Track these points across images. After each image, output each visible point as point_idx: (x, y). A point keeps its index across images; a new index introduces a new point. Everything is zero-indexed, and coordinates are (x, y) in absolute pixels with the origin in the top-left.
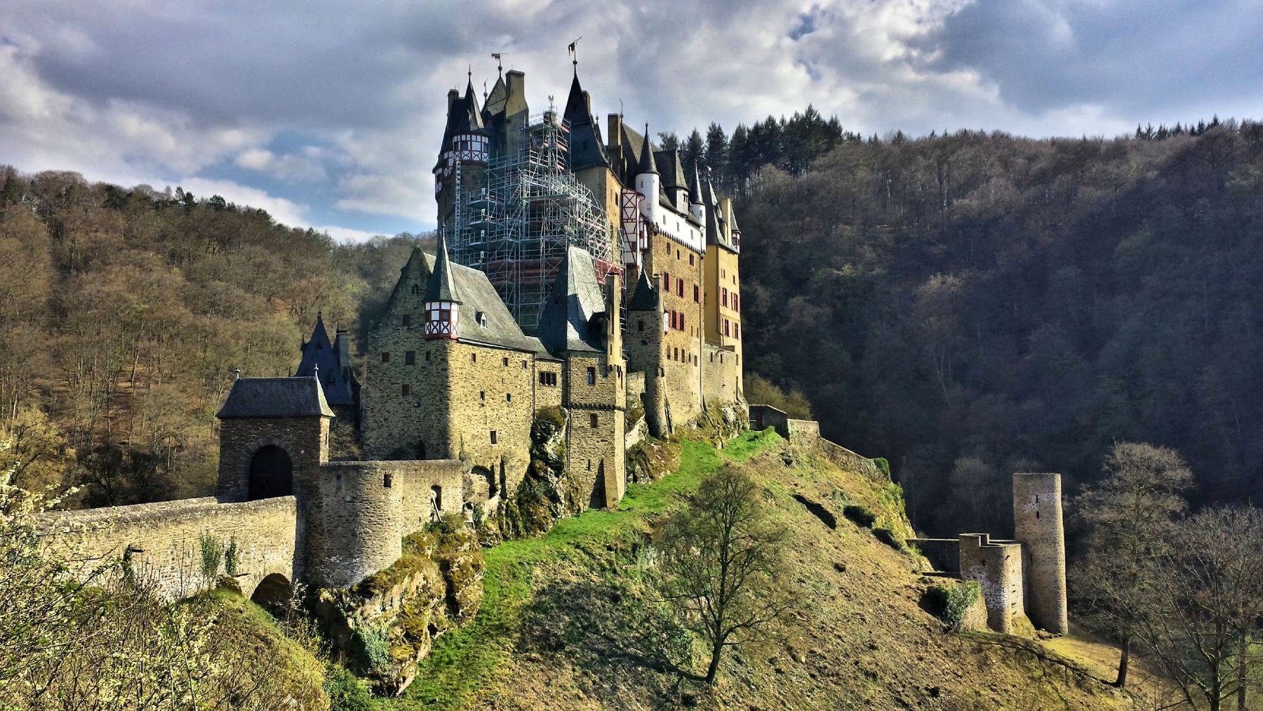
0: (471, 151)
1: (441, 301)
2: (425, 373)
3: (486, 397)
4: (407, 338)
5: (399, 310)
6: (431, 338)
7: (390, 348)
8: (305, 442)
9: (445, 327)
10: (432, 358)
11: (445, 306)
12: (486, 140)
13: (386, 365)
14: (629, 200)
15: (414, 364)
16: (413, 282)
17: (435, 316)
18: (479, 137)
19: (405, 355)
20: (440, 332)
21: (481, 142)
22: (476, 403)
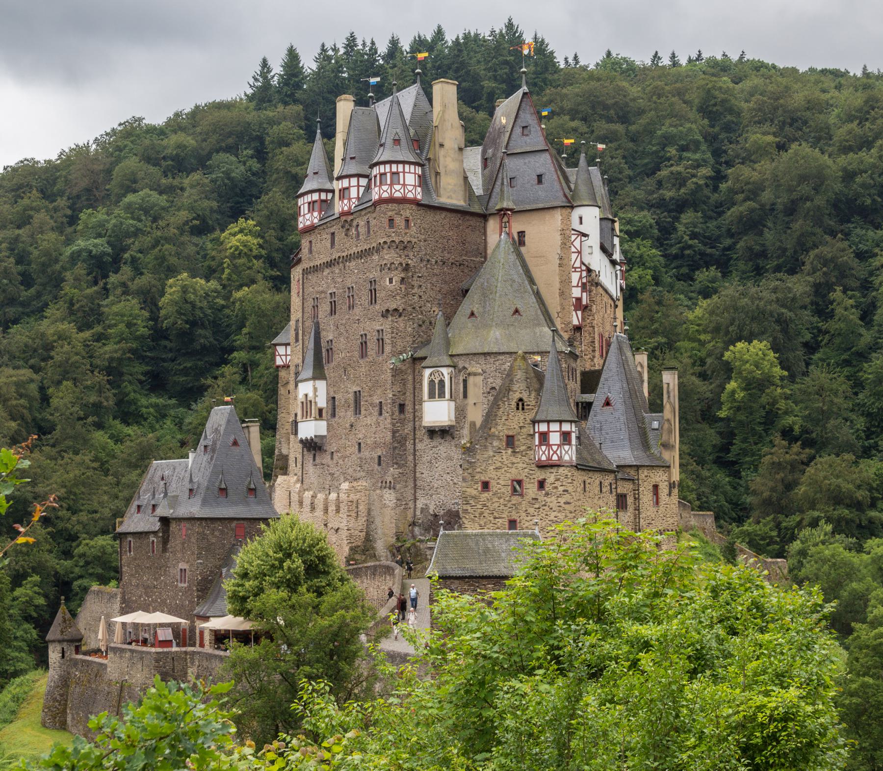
0: (404, 185)
1: (561, 422)
2: (537, 506)
4: (513, 463)
5: (501, 429)
6: (542, 466)
7: (490, 475)
9: (567, 452)
10: (548, 487)
11: (566, 427)
12: (419, 170)
13: (486, 495)
15: (522, 495)
16: (517, 396)
17: (555, 438)
18: (412, 167)
19: (510, 482)
20: (560, 458)
21: (415, 173)
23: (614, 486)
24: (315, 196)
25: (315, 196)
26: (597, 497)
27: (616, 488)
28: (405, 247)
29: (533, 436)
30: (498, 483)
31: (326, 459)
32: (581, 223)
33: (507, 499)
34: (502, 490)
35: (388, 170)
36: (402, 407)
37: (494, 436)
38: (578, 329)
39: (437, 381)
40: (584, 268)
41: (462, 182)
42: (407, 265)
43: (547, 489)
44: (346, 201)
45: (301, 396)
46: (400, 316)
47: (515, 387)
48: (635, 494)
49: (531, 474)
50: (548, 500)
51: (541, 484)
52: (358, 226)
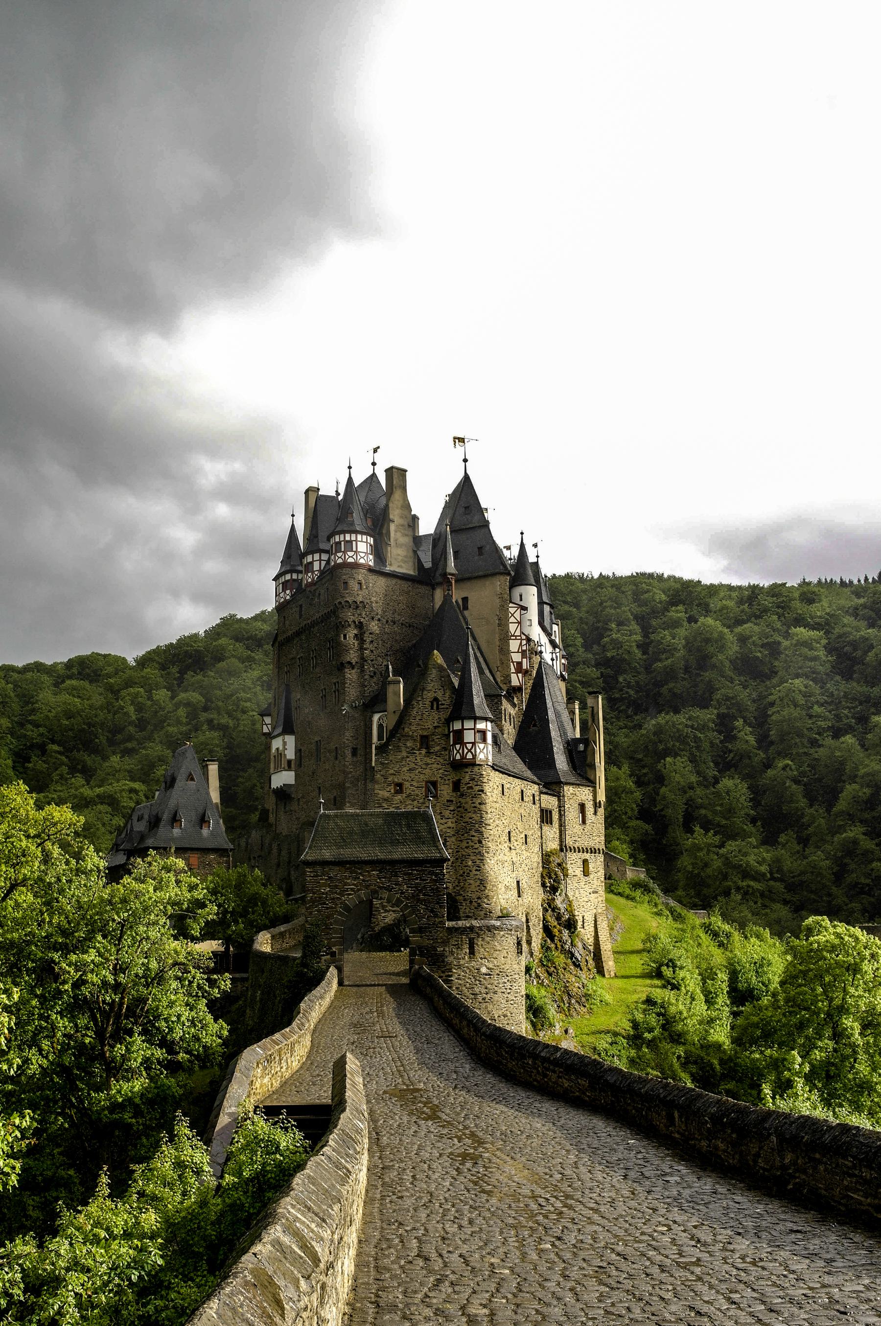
0: (356, 552)
1: (475, 719)
2: (452, 808)
3: (512, 839)
4: (427, 764)
5: (414, 728)
8: (424, 895)
10: (464, 788)
11: (481, 725)
12: (371, 540)
13: (399, 797)
14: (512, 615)
17: (469, 737)
18: (364, 537)
21: (367, 542)
22: (506, 845)
23: (537, 798)
24: (288, 577)
25: (288, 577)
26: (518, 805)
27: (540, 800)
28: (357, 607)
29: (448, 736)
30: (411, 785)
31: (294, 806)
32: (521, 600)
33: (421, 801)
34: (416, 792)
35: (342, 539)
36: (354, 752)
37: (409, 736)
38: (519, 689)
39: (384, 725)
40: (524, 637)
41: (411, 554)
42: (360, 623)
43: (462, 790)
44: (309, 574)
45: (273, 750)
46: (353, 668)
47: (430, 686)
48: (560, 811)
49: (446, 775)
50: (463, 801)
51: (456, 786)
52: (319, 594)
